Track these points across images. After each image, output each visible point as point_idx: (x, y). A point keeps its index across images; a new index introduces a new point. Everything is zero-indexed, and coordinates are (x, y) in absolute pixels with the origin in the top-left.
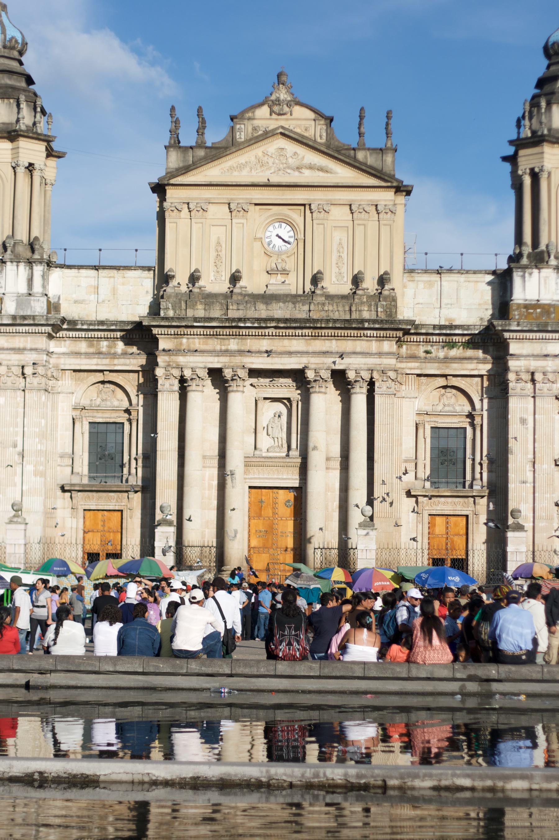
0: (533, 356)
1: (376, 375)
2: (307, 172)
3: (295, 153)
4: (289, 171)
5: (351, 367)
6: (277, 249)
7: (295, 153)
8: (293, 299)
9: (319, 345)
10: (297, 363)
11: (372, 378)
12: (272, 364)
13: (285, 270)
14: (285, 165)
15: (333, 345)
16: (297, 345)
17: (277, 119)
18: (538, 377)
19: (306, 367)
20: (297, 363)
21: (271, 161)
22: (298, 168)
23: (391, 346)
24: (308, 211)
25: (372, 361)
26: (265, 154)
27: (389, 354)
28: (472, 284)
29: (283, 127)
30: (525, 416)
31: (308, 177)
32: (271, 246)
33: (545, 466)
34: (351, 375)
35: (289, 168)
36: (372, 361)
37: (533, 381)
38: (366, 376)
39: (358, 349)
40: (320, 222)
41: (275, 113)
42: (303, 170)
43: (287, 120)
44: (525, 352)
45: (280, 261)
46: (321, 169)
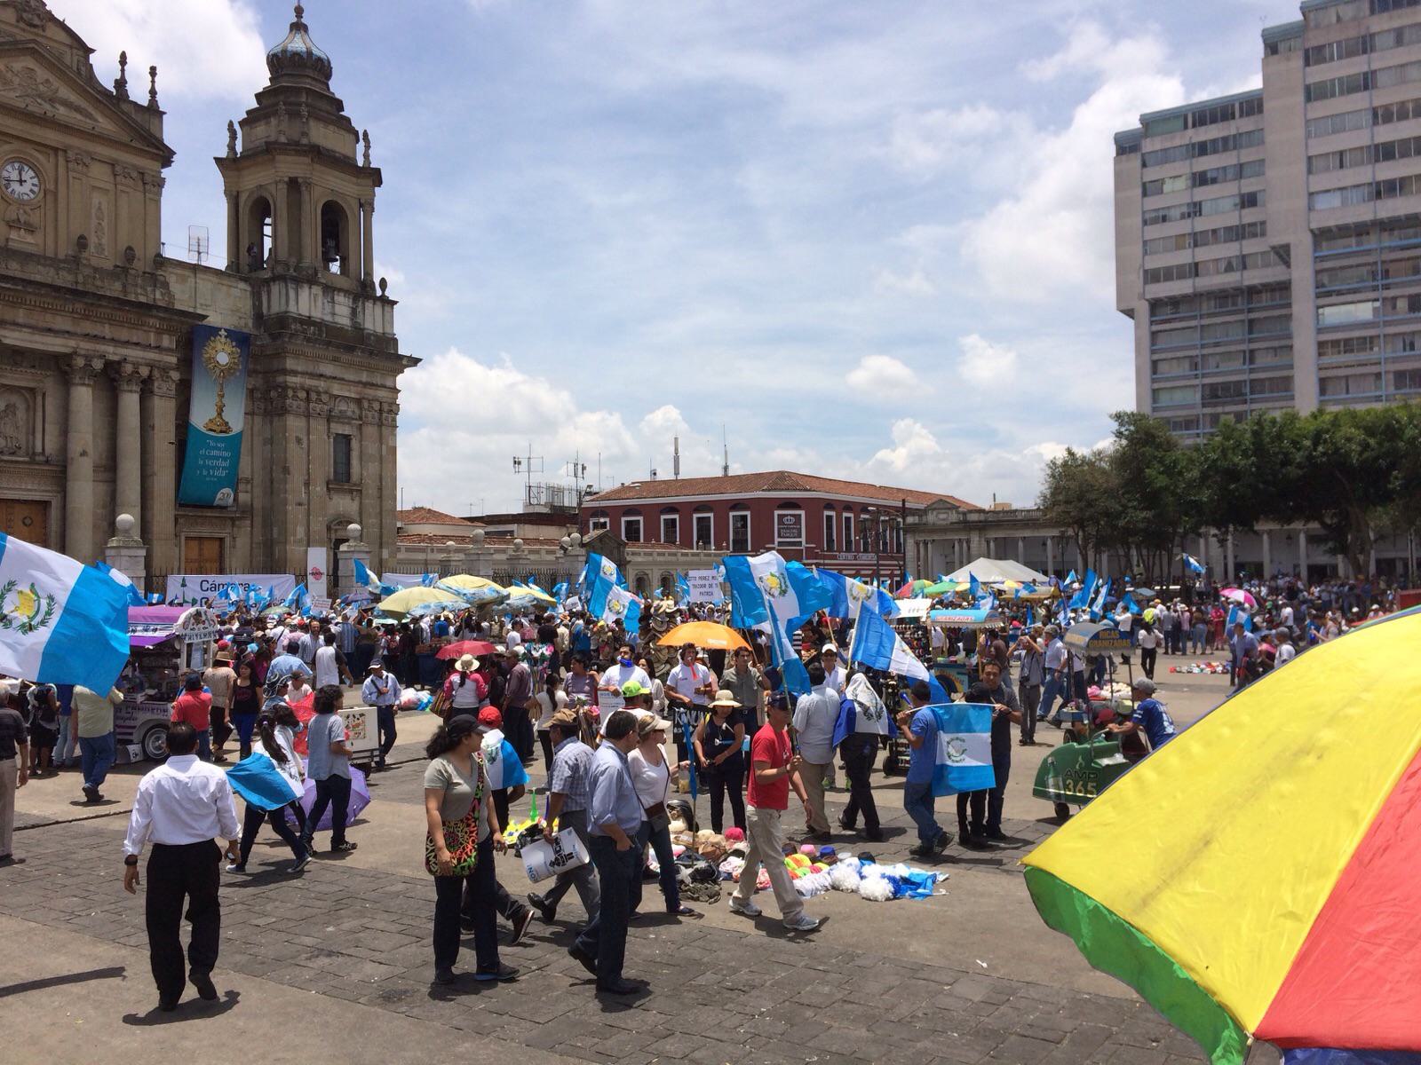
0: (307, 373)
1: (156, 373)
2: (62, 110)
3: (47, 81)
4: (39, 101)
5: (129, 359)
6: (16, 196)
7: (47, 81)
8: (53, 262)
9: (88, 327)
10: (63, 346)
11: (150, 377)
12: (31, 342)
13: (31, 225)
14: (34, 92)
15: (107, 331)
16: (61, 323)
17: (24, 30)
18: (314, 396)
19: (75, 353)
20: (63, 346)
21: (17, 80)
22: (52, 101)
23: (171, 341)
24: (61, 160)
25: (152, 355)
26: (9, 69)
27: (169, 350)
28: (225, 288)
29: (34, 41)
30: (301, 436)
31: (62, 112)
32: (10, 190)
33: (318, 489)
34: (129, 368)
35: (40, 96)
36: (152, 355)
37: (308, 399)
38: (144, 372)
39: (135, 340)
40: (78, 176)
41: (25, 21)
42: (57, 106)
43: (37, 35)
44: (300, 369)
45: (21, 211)
46: (78, 109)
